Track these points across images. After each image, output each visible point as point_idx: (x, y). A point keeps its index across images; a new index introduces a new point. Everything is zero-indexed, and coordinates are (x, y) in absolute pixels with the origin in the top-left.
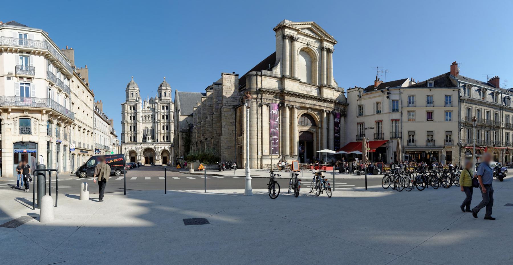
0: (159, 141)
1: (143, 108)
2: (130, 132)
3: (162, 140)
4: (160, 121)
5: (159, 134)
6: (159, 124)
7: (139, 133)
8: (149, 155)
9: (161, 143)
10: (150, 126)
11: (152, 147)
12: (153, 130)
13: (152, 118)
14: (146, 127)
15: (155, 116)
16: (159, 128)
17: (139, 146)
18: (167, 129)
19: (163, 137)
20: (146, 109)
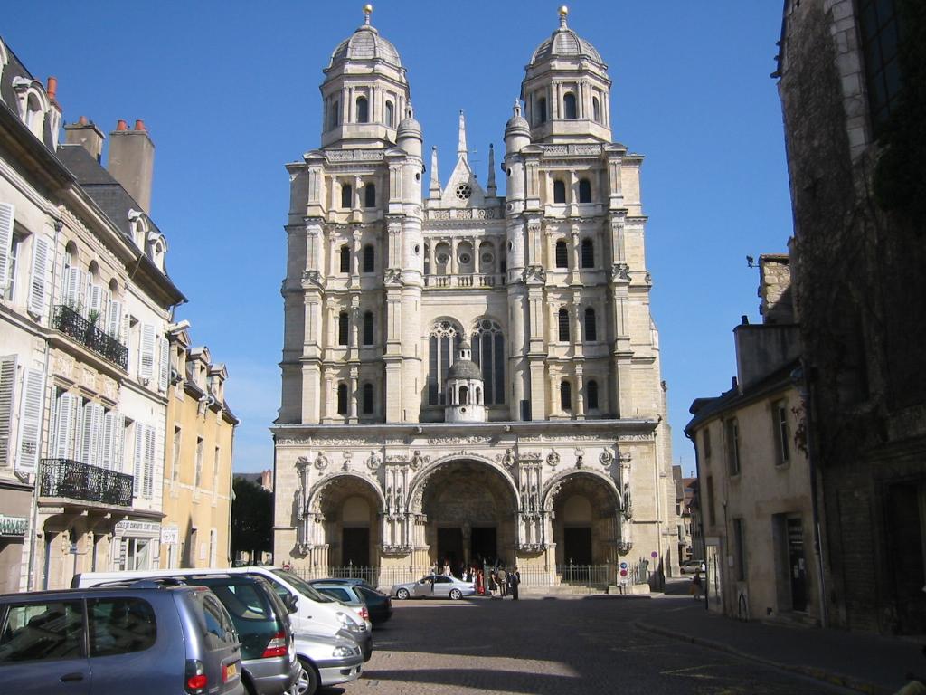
0: (538, 413)
1: (426, 199)
2: (336, 355)
3: (557, 408)
4: (541, 274)
5: (537, 367)
6: (535, 293)
7: (399, 359)
8: (462, 513)
9: (552, 430)
10: (470, 312)
11: (491, 455)
12: (494, 349)
13: (485, 258)
14: (447, 322)
15: (505, 246)
16: (539, 324)
17: (396, 451)
18: (590, 334)
19: (566, 387)
20: (450, 198)
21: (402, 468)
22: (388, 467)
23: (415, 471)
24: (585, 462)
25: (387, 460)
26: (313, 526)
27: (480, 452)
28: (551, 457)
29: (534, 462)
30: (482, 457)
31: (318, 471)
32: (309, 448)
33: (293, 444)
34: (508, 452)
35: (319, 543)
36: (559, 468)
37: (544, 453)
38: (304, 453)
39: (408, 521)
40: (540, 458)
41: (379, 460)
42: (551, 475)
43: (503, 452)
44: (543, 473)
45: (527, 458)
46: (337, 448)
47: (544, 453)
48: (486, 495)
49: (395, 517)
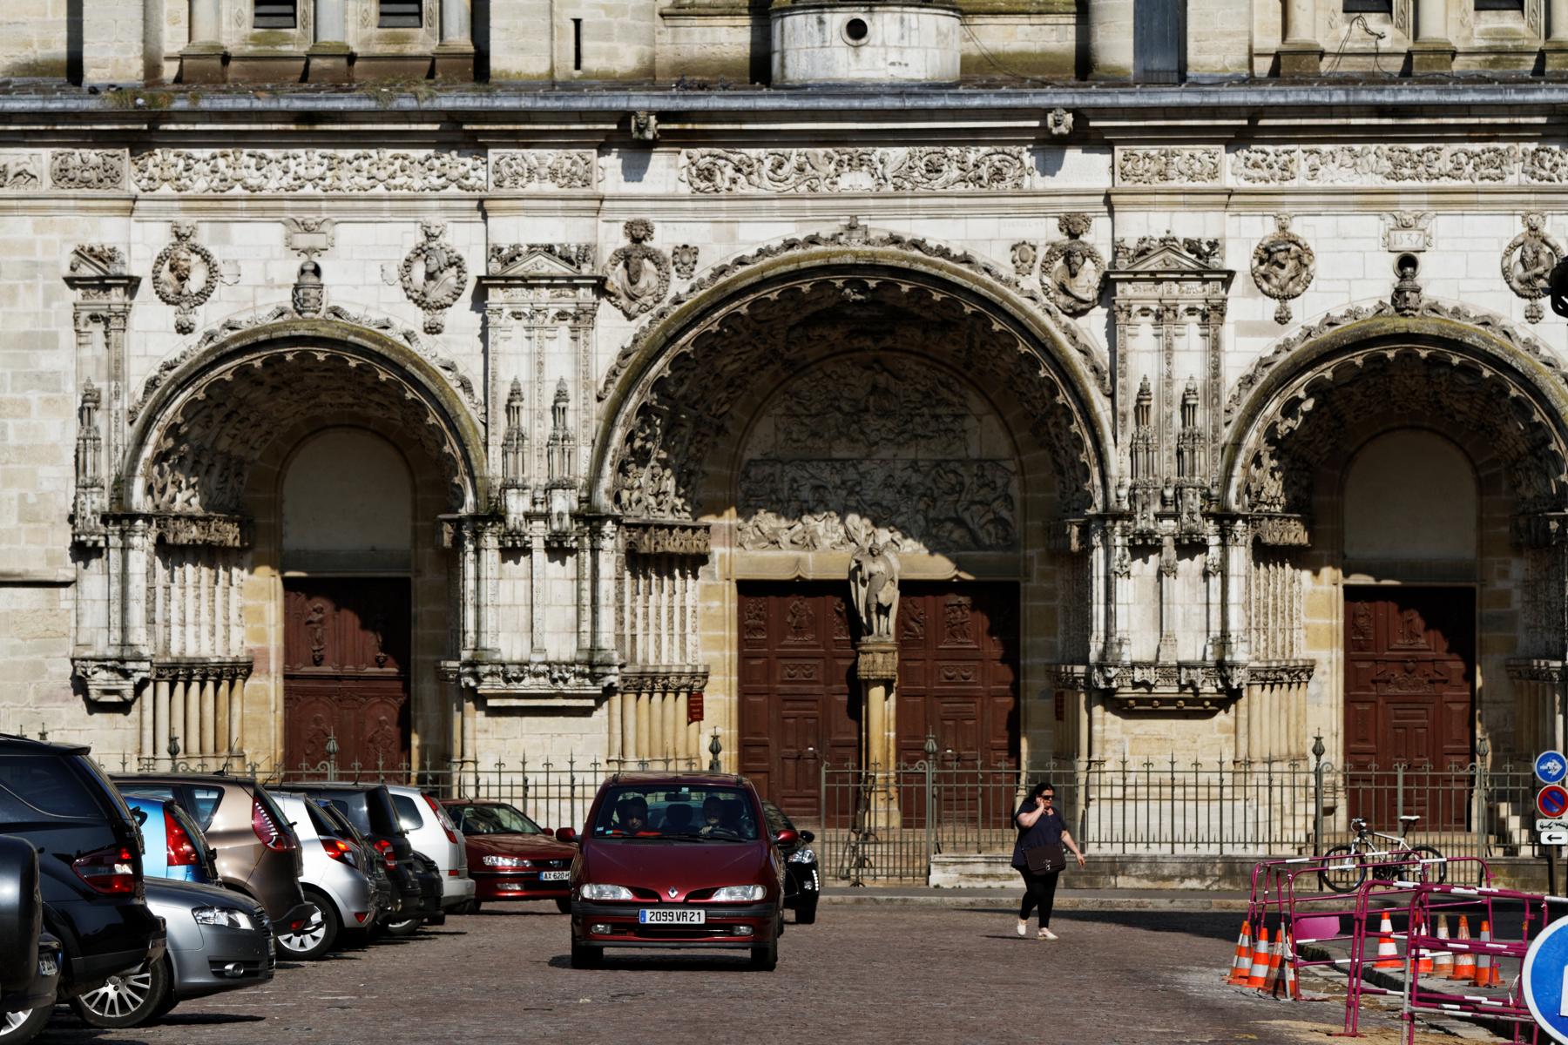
21: (568, 300)
22: (496, 297)
23: (630, 317)
24: (1434, 283)
25: (496, 268)
26: (151, 573)
27: (935, 232)
28: (1267, 256)
29: (1181, 276)
30: (945, 253)
31: (169, 315)
32: (130, 206)
33: (46, 185)
34: (1072, 227)
35: (175, 650)
36: (1309, 310)
37: (1240, 239)
38: (106, 231)
39: (595, 551)
40: (1214, 262)
41: (457, 263)
42: (1264, 346)
43: (1044, 232)
44: (1228, 331)
45: (1154, 263)
46: (258, 202)
47: (1240, 239)
48: (970, 423)
49: (538, 534)
